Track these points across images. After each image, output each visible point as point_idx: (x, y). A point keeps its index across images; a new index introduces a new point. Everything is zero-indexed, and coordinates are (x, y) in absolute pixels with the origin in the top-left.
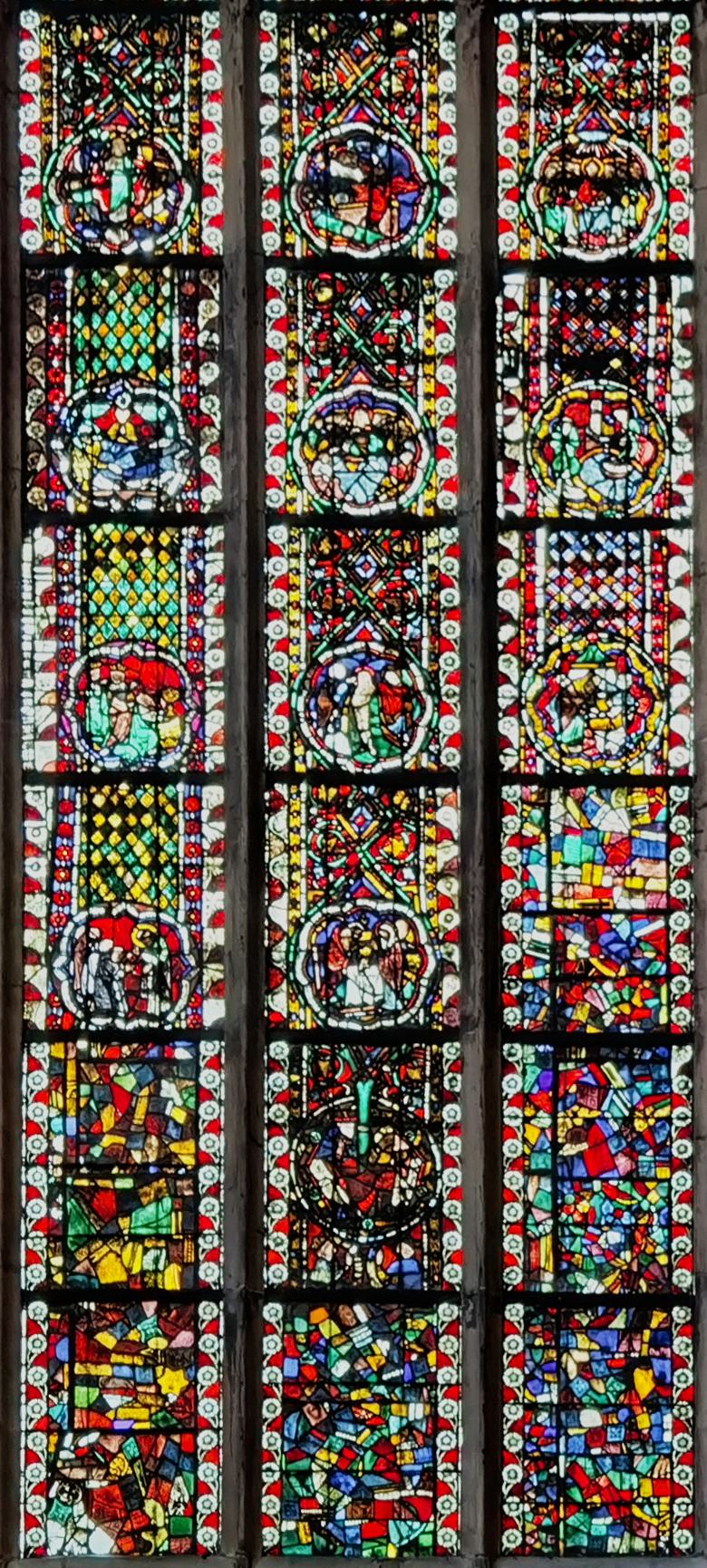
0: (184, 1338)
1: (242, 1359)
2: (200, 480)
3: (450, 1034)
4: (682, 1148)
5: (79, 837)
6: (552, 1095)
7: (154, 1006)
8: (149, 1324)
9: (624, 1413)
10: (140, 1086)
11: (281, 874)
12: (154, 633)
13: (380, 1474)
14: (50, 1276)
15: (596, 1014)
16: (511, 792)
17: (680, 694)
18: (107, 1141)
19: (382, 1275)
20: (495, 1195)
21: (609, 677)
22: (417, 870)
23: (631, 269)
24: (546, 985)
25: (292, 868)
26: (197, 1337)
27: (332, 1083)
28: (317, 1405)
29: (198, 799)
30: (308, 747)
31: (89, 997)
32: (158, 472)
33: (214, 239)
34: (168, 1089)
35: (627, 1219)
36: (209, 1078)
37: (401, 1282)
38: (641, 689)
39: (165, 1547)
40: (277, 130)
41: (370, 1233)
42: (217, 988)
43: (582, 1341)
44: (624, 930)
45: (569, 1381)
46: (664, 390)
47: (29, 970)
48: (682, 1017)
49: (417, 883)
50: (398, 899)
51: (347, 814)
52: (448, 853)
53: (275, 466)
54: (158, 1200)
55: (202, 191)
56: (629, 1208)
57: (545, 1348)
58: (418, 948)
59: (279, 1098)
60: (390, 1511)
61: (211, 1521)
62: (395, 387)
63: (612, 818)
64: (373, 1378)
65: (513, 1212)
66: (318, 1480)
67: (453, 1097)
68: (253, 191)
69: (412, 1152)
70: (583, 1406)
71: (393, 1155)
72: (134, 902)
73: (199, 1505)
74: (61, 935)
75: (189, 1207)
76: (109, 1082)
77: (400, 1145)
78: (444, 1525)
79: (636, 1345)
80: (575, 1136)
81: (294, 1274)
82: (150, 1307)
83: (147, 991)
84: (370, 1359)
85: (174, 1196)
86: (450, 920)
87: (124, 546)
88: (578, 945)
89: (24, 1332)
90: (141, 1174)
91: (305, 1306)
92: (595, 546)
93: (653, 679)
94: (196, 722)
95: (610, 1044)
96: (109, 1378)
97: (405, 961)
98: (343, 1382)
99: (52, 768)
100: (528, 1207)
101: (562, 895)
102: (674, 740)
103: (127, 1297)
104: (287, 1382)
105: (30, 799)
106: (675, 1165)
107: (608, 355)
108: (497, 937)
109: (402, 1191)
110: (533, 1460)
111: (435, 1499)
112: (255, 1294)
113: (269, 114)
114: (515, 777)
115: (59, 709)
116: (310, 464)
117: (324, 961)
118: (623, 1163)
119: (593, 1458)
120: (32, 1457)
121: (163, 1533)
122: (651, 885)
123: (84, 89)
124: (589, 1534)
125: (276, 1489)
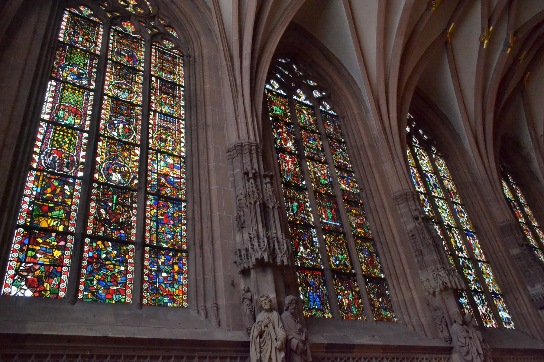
0: (62, 243)
7: (65, 170)
8: (53, 238)
9: (172, 274)
10: (59, 185)
12: (76, 104)
13: (112, 282)
14: (26, 223)
15: (166, 193)
17: (182, 144)
18: (48, 195)
19: (116, 236)
22: (130, 159)
24: (156, 185)
25: (102, 152)
26: (66, 243)
27: (108, 194)
28: (97, 263)
29: (82, 135)
30: (108, 132)
31: (49, 164)
32: (82, 80)
34: (66, 187)
35: (172, 233)
36: (77, 187)
37: (121, 238)
39: (49, 296)
41: (114, 227)
43: (163, 257)
44: (172, 180)
45: (159, 265)
47: (34, 156)
48: (184, 197)
49: (130, 161)
50: (125, 163)
51: (116, 146)
53: (106, 87)
54: (60, 210)
56: (173, 231)
57: (154, 258)
58: (129, 173)
61: (64, 290)
63: (170, 161)
64: (112, 259)
65: (148, 228)
66: (95, 282)
69: (125, 211)
70: (163, 272)
71: (120, 211)
72: (64, 149)
73: (61, 286)
74: (44, 151)
75: (68, 214)
78: (128, 297)
79: (175, 260)
80: (162, 215)
81: (93, 233)
83: (64, 167)
84: (111, 255)
85: (64, 210)
87: (72, 89)
88: (163, 180)
89: (15, 235)
90: (56, 204)
91: (96, 240)
92: (167, 119)
94: (83, 122)
95: (168, 199)
96: (39, 250)
97: (126, 175)
98: (104, 259)
99: (48, 120)
100: (151, 227)
101: (160, 171)
102: (182, 151)
103: (48, 231)
105: (41, 124)
107: (170, 93)
109: (122, 219)
110: (150, 283)
111: (126, 290)
115: (52, 110)
116: (114, 89)
117: (108, 170)
118: (172, 222)
119: (165, 284)
120: (11, 268)
121: (49, 292)
122: (177, 173)
124: (163, 301)
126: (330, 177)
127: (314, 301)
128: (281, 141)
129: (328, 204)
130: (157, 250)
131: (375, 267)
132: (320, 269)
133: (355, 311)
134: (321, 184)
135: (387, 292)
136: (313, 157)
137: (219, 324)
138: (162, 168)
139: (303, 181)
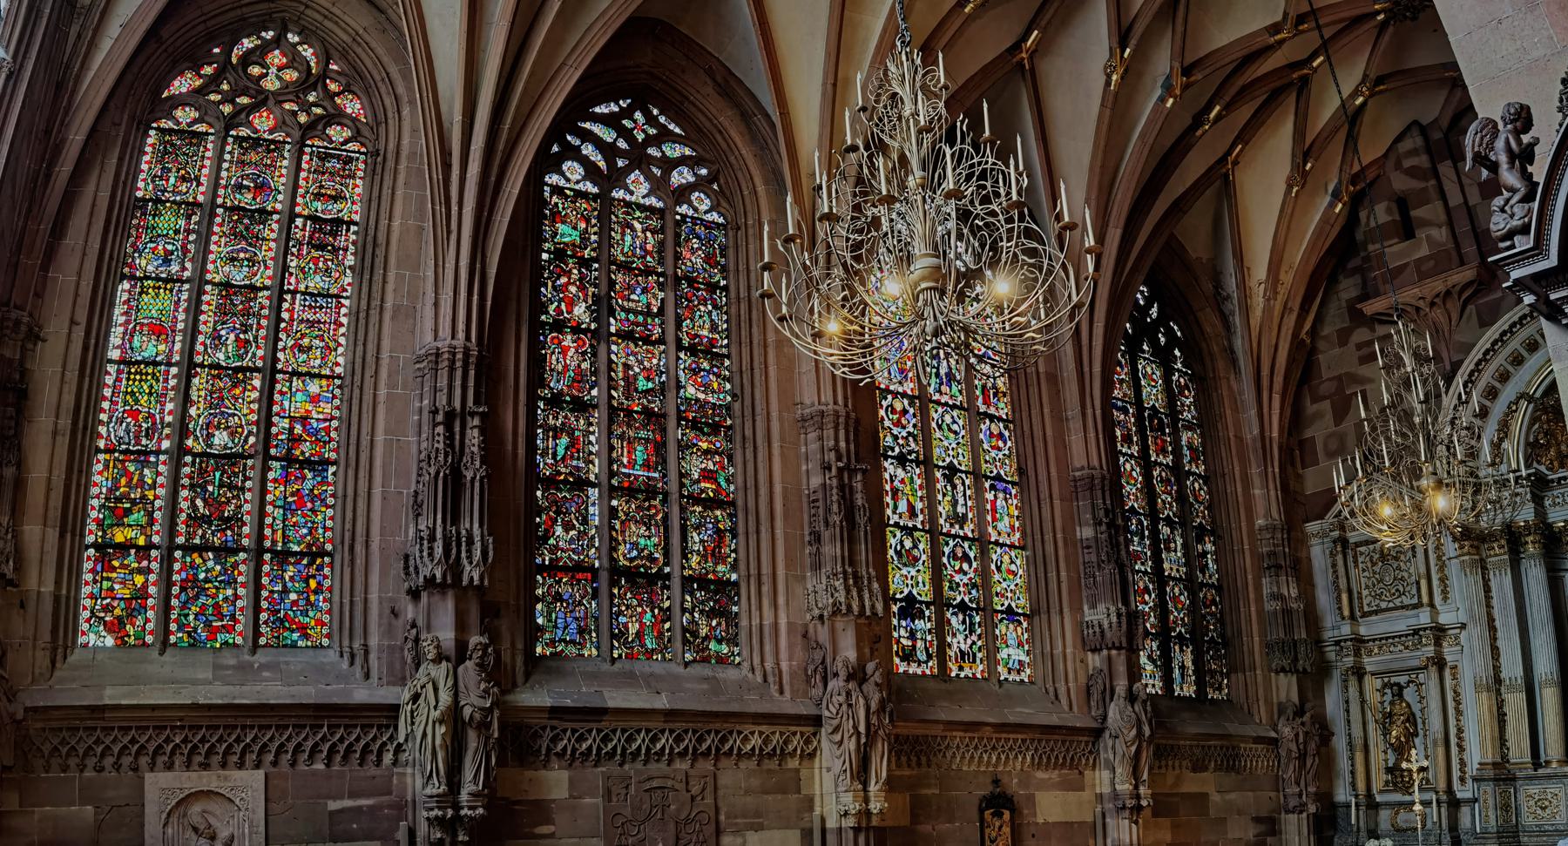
0: (145, 563)
1: (167, 570)
2: (184, 269)
3: (250, 457)
4: (330, 501)
5: (124, 382)
6: (285, 480)
7: (144, 442)
8: (132, 558)
11: (195, 398)
16: (279, 376)
17: (340, 350)
20: (262, 514)
21: (317, 342)
23: (338, 222)
33: (201, 198)
34: (146, 471)
36: (162, 468)
38: (328, 347)
40: (227, 170)
42: (168, 437)
46: (345, 257)
52: (255, 395)
55: (199, 184)
59: (186, 476)
60: (218, 630)
62: (255, 247)
66: (191, 617)
67: (250, 479)
68: (216, 185)
75: (150, 514)
76: (125, 468)
77: (229, 495)
81: (187, 540)
82: (133, 551)
86: (254, 417)
90: (133, 502)
93: (332, 345)
102: (338, 364)
103: (124, 548)
104: (182, 580)
106: (328, 507)
108: (270, 424)
112: (172, 547)
113: (225, 165)
114: (281, 371)
117: (207, 429)
123: (166, 152)
125: (176, 621)
126: (662, 373)
127: (565, 628)
128: (558, 306)
129: (642, 434)
130: (283, 557)
131: (719, 559)
132: (592, 569)
133: (650, 643)
134: (636, 390)
135: (735, 609)
136: (632, 331)
137: (367, 676)
138: (298, 405)
139: (592, 388)
